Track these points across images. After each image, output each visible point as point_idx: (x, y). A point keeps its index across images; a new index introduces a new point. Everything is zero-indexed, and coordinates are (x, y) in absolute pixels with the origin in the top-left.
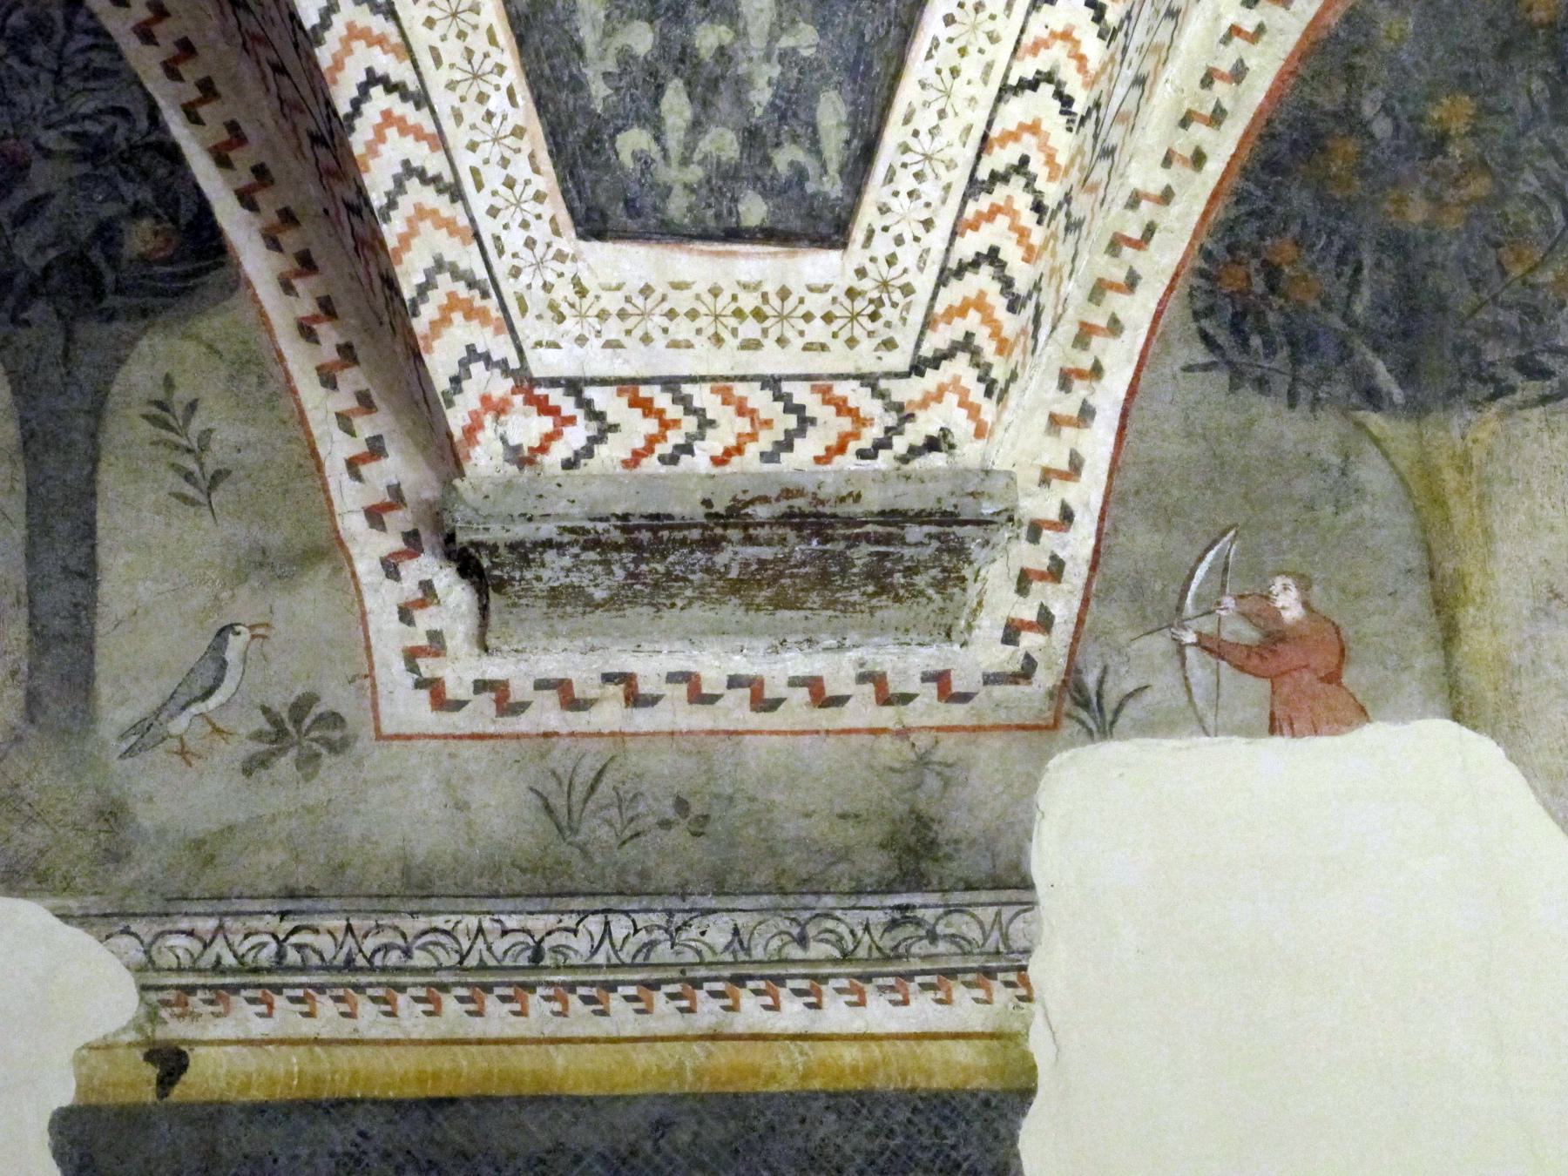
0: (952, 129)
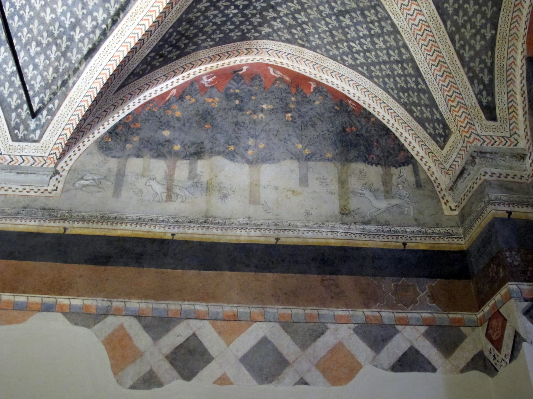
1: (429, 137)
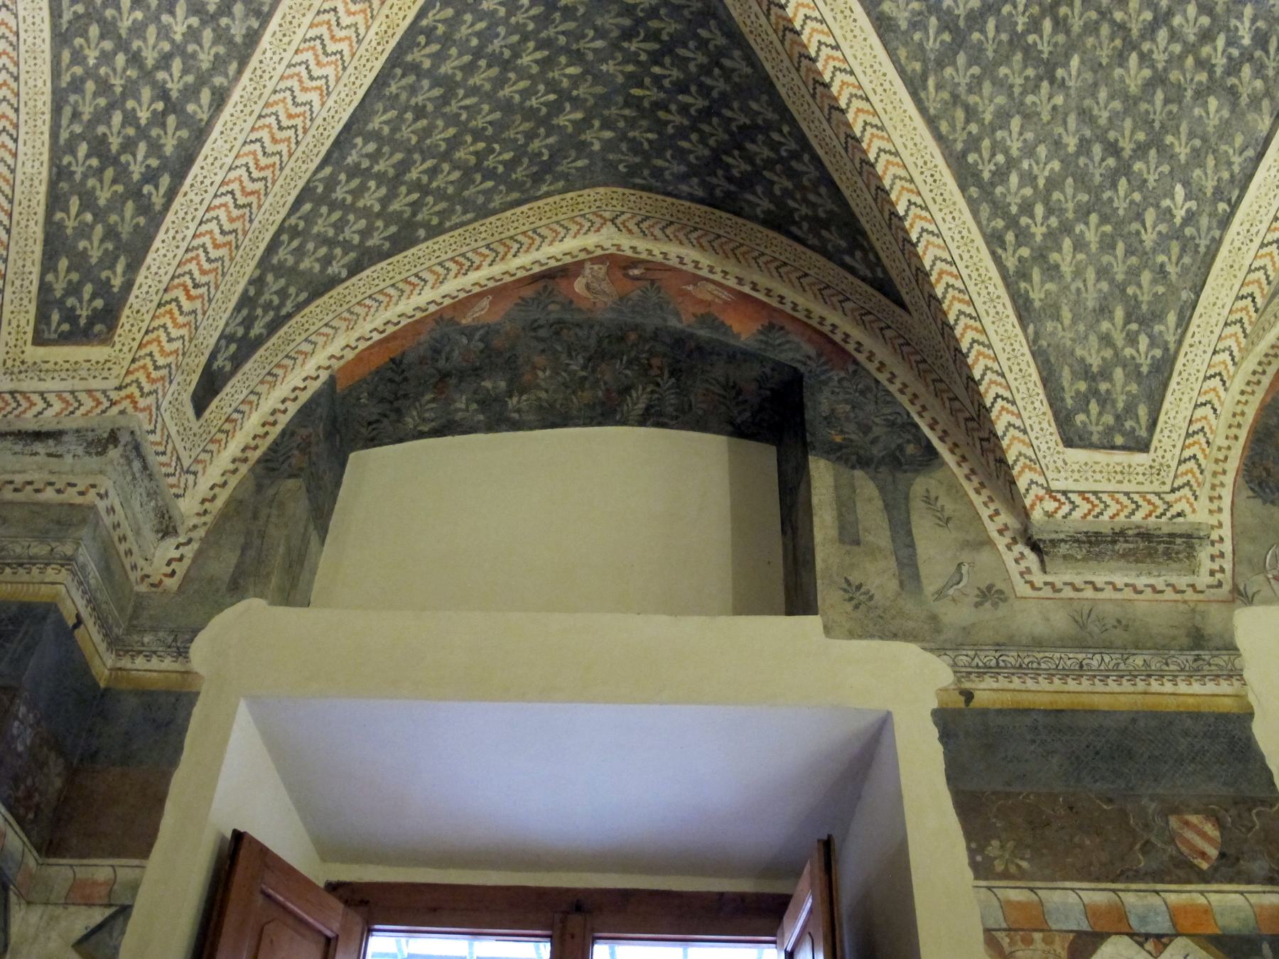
0: (1180, 417)
1: (34, 288)
